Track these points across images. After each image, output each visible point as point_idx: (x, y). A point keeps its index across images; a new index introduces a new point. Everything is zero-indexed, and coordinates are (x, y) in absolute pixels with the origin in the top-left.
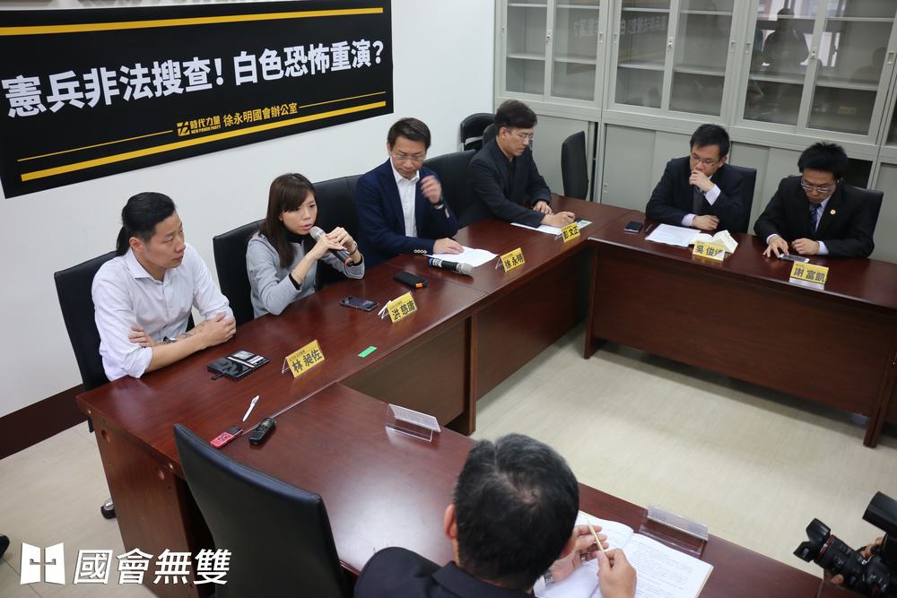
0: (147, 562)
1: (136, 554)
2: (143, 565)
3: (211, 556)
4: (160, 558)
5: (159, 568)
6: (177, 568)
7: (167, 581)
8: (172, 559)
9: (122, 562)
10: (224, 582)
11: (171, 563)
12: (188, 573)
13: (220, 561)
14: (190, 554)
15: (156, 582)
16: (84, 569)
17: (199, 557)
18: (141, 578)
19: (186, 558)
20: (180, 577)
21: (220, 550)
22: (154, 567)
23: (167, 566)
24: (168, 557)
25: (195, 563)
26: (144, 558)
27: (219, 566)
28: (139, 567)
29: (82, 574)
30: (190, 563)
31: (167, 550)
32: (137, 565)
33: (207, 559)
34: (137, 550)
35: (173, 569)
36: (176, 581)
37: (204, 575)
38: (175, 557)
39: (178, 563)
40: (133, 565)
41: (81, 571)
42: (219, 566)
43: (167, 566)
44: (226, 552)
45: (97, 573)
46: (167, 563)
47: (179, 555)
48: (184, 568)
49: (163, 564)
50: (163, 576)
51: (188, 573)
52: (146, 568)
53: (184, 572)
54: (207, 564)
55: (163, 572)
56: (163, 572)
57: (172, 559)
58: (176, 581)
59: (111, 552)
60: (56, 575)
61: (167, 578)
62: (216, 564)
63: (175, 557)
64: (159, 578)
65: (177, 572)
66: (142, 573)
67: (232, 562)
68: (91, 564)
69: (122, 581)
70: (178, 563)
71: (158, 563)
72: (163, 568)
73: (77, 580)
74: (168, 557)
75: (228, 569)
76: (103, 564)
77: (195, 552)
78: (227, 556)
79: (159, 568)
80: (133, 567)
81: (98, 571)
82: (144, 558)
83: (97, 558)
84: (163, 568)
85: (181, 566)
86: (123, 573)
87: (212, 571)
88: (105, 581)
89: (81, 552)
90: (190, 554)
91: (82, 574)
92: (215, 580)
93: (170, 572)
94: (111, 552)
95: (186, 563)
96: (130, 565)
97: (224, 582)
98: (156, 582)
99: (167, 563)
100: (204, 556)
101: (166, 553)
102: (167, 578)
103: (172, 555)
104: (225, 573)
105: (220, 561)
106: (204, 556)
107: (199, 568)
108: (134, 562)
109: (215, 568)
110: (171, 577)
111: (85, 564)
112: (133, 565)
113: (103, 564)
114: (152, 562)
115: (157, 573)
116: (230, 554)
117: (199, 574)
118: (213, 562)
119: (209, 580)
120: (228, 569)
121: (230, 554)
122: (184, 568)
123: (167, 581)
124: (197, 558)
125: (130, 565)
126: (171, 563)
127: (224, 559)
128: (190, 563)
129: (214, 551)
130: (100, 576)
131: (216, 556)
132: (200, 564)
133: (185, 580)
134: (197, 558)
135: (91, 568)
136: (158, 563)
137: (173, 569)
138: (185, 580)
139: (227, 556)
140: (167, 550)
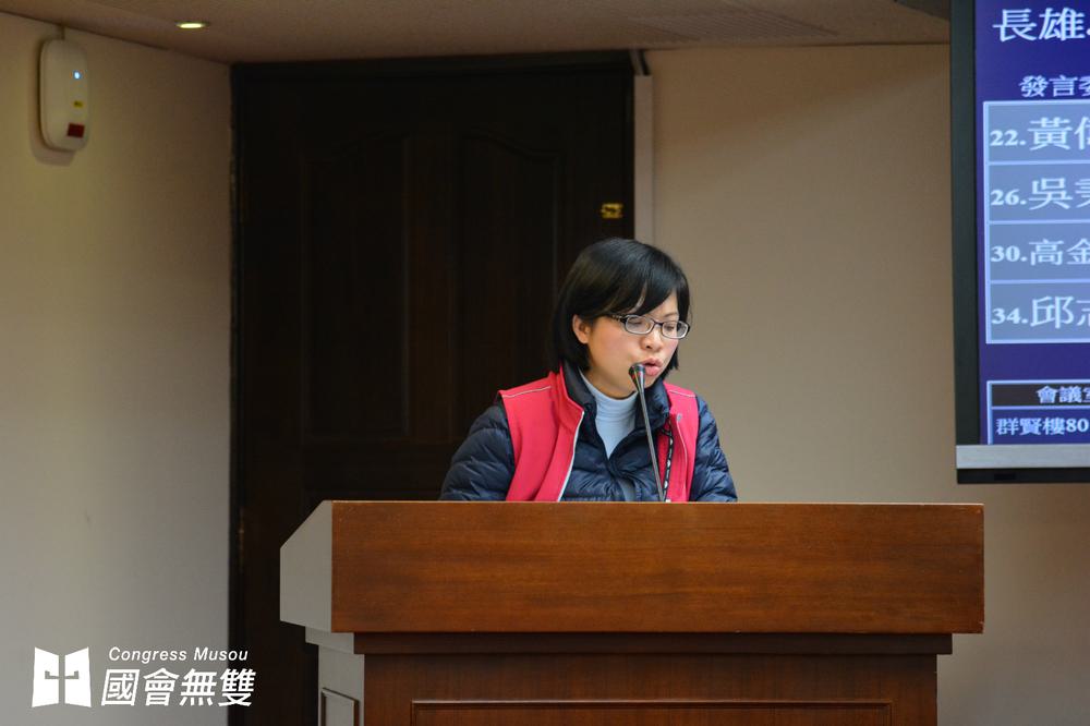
0: (173, 683)
1: (162, 674)
2: (169, 685)
3: (236, 676)
4: (186, 678)
5: (185, 689)
6: (202, 689)
7: (192, 703)
8: (197, 679)
9: (148, 683)
10: (248, 704)
11: (196, 684)
12: (213, 694)
13: (244, 682)
14: (215, 674)
15: (182, 703)
16: (111, 690)
17: (224, 677)
18: (167, 699)
19: (211, 679)
20: (205, 698)
21: (244, 670)
22: (179, 688)
23: (192, 687)
24: (194, 678)
25: (220, 683)
26: (170, 679)
27: (244, 687)
28: (165, 688)
29: (110, 696)
30: (215, 684)
31: (193, 670)
32: (163, 685)
33: (232, 679)
34: (163, 670)
35: (199, 690)
36: (201, 702)
37: (229, 696)
38: (201, 678)
39: (203, 684)
40: (160, 685)
41: (108, 692)
42: (244, 687)
43: (192, 687)
44: (251, 673)
45: (124, 694)
46: (193, 684)
47: (204, 675)
48: (209, 689)
49: (189, 684)
50: (189, 697)
51: (213, 694)
52: (172, 689)
53: (209, 693)
54: (232, 684)
55: (188, 693)
56: (188, 693)
57: (197, 679)
58: (201, 702)
59: (137, 672)
60: (79, 694)
61: (192, 700)
62: (241, 684)
63: (201, 678)
64: (185, 699)
65: (202, 693)
66: (168, 695)
67: (257, 682)
68: (118, 684)
69: (148, 703)
70: (203, 684)
71: (184, 684)
72: (189, 688)
73: (104, 703)
74: (194, 678)
75: (252, 690)
76: (130, 685)
77: (221, 673)
78: (251, 682)
79: (185, 689)
80: (159, 688)
81: (125, 691)
82: (170, 679)
83: (124, 679)
84: (189, 688)
85: (206, 687)
86: (149, 695)
87: (237, 692)
88: (132, 703)
89: (109, 672)
90: (215, 674)
91: (110, 696)
92: (240, 702)
93: (195, 693)
94: (137, 672)
95: (211, 684)
96: (157, 685)
97: (248, 704)
98: (182, 703)
99: (193, 684)
100: (229, 676)
101: (192, 672)
102: (192, 700)
103: (198, 675)
104: (249, 695)
105: (244, 682)
106: (229, 676)
107: (224, 689)
108: (160, 683)
109: (240, 689)
110: (196, 698)
111: (112, 684)
112: (160, 685)
113: (130, 685)
114: (178, 682)
115: (183, 694)
116: (254, 674)
117: (224, 695)
118: (238, 682)
119: (234, 702)
120: (252, 690)
121: (254, 674)
122: (209, 689)
123: (192, 703)
124: (222, 678)
125: (157, 685)
126: (196, 684)
127: (248, 679)
128: (215, 684)
129: (239, 671)
130: (127, 697)
131: (241, 677)
132: (225, 684)
133: (210, 702)
134: (222, 678)
135: (117, 690)
136: (184, 684)
137: (199, 690)
138: (210, 702)
139: (251, 682)
140: (193, 670)
